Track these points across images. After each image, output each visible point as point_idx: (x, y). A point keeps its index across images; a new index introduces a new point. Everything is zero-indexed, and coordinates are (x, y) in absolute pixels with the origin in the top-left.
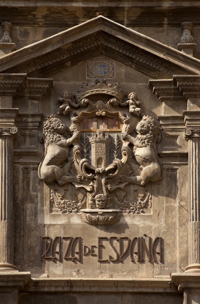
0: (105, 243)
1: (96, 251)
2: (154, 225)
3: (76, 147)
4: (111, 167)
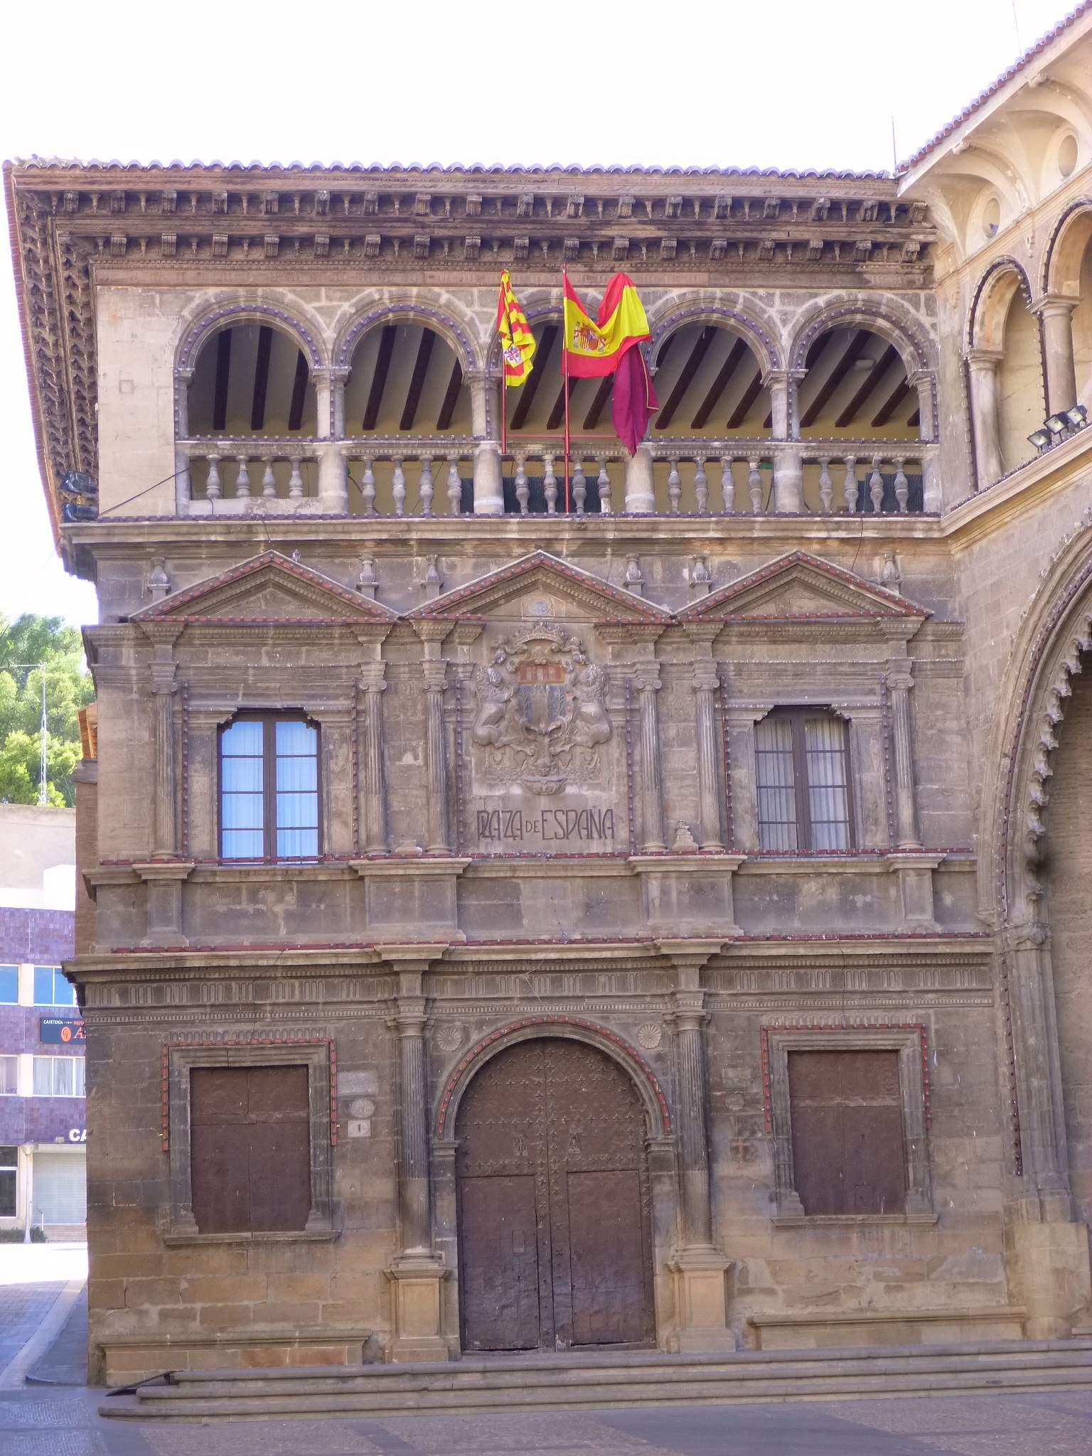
0: (547, 816)
1: (539, 825)
2: (604, 795)
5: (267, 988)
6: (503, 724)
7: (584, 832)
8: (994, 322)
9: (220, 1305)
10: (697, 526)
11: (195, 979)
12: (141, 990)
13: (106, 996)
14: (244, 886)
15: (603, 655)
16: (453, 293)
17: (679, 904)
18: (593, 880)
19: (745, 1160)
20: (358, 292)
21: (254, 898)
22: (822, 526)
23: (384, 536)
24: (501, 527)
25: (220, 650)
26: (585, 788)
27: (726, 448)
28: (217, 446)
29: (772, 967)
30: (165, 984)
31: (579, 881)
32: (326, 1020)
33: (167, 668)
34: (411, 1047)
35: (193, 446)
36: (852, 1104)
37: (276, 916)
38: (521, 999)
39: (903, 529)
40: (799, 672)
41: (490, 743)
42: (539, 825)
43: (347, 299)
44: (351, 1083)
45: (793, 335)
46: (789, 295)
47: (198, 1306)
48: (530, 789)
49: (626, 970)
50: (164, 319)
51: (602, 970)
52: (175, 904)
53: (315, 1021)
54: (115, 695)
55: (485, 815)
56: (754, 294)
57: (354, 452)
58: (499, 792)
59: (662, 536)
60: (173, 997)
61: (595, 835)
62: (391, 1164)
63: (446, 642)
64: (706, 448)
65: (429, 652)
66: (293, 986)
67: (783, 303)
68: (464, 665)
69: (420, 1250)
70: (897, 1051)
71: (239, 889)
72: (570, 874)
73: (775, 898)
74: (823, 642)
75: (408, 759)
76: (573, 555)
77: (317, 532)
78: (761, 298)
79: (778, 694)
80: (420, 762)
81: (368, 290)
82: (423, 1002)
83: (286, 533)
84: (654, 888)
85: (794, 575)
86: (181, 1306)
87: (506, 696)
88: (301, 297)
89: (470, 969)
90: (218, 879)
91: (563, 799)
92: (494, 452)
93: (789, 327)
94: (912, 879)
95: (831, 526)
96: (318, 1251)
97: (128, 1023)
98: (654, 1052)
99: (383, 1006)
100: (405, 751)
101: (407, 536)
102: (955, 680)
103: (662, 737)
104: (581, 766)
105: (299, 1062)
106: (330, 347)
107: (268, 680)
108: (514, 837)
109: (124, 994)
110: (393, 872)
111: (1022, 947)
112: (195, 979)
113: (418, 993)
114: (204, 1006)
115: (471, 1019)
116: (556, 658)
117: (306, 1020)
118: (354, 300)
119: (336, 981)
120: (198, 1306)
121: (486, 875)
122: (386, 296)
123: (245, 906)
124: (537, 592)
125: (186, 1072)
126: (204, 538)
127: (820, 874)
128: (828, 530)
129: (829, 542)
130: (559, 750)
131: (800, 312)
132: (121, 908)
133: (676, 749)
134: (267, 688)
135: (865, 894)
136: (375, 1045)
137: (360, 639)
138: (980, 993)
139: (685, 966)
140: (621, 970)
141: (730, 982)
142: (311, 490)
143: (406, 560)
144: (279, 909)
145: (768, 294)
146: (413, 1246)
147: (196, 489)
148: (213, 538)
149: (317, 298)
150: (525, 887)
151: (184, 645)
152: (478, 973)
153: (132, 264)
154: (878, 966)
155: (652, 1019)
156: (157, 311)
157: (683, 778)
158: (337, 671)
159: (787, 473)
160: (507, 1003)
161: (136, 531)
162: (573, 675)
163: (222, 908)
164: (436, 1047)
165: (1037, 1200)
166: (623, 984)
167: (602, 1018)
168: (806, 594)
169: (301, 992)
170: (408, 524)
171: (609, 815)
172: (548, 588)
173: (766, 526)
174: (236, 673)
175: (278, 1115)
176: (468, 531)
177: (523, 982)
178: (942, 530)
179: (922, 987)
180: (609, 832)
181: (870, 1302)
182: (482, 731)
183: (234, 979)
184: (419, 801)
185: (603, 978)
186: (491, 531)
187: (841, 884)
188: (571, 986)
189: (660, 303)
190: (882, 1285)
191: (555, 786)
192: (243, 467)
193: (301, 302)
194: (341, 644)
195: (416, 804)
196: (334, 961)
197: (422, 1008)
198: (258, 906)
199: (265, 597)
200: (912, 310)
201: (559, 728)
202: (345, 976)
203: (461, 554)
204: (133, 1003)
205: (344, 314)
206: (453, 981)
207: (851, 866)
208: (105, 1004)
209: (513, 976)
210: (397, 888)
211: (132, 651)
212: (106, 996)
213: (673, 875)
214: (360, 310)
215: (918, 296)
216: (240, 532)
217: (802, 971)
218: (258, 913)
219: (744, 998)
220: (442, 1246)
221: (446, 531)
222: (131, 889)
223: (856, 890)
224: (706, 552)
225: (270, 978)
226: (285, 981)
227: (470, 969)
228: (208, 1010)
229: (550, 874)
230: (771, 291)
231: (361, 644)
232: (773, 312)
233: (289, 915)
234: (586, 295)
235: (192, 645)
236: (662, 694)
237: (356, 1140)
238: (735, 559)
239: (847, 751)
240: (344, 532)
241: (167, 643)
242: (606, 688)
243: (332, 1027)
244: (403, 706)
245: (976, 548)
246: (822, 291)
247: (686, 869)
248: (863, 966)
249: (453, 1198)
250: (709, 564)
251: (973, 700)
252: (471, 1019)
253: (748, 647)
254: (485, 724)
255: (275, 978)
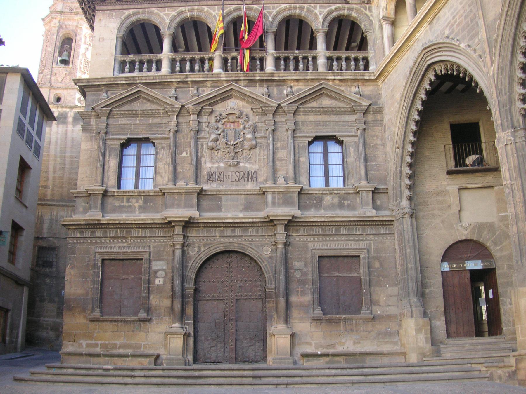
0: (233, 174)
1: (230, 177)
2: (254, 167)
3: (222, 134)
4: (236, 142)
5: (130, 231)
6: (218, 142)
7: (246, 179)
8: (390, 8)
9: (107, 342)
10: (288, 75)
11: (105, 228)
12: (87, 232)
13: (75, 233)
14: (125, 197)
15: (254, 119)
16: (209, 8)
17: (278, 203)
18: (248, 196)
19: (301, 295)
20: (178, 9)
21: (128, 201)
22: (331, 74)
23: (179, 80)
24: (219, 75)
25: (123, 119)
26: (247, 164)
27: (300, 53)
28: (129, 57)
29: (313, 226)
30: (95, 230)
31: (243, 196)
32: (150, 243)
33: (103, 124)
34: (178, 252)
35: (121, 57)
36: (342, 275)
37: (135, 207)
38: (220, 236)
39: (361, 76)
40: (325, 124)
41: (213, 149)
42: (230, 177)
43: (174, 11)
44: (156, 265)
45: (324, 18)
46: (322, 6)
47: (100, 342)
48: (227, 164)
49: (258, 226)
50: (115, 19)
51: (250, 226)
52: (100, 202)
53: (146, 243)
54: (88, 134)
55: (210, 173)
56: (310, 6)
57: (175, 57)
58: (216, 165)
59: (276, 78)
60: (98, 234)
61: (250, 180)
62: (170, 294)
63: (199, 114)
64: (294, 53)
65: (194, 117)
66: (139, 231)
67: (320, 8)
68: (205, 122)
69: (177, 325)
70: (359, 256)
71: (123, 198)
72: (240, 193)
73: (315, 202)
74: (334, 114)
75: (184, 154)
76: (245, 86)
77: (155, 79)
78: (312, 7)
79: (317, 132)
80: (188, 155)
81: (181, 8)
82: (182, 236)
83: (146, 79)
84: (270, 197)
85: (323, 92)
86: (93, 342)
87: (219, 132)
88: (159, 11)
89: (202, 226)
90: (116, 194)
91: (239, 168)
92: (220, 55)
93: (322, 15)
94: (364, 194)
95: (336, 74)
96: (142, 325)
97: (82, 243)
98: (268, 256)
99: (170, 238)
100: (183, 152)
101: (187, 80)
102: (381, 127)
103: (275, 146)
104: (246, 157)
105: (140, 257)
106: (168, 25)
107: (138, 129)
108: (221, 181)
109: (81, 233)
110: (175, 191)
111: (404, 216)
112: (105, 228)
113: (181, 233)
114: (107, 237)
115: (202, 243)
116: (237, 120)
117: (142, 243)
118: (176, 11)
119: (154, 229)
120: (100, 342)
121: (209, 193)
122: (187, 9)
123: (125, 204)
124: (232, 99)
125: (100, 260)
126: (119, 82)
127: (331, 193)
128: (334, 76)
129: (335, 81)
130: (237, 151)
131: (325, 11)
132: (83, 204)
133: (280, 150)
134: (138, 131)
135: (348, 200)
136: (166, 252)
137: (169, 114)
138: (390, 235)
139: (279, 224)
140: (257, 226)
141: (297, 231)
142: (158, 69)
143: (187, 89)
144: (136, 205)
145: (315, 6)
146: (175, 323)
147: (122, 70)
148: (122, 82)
149: (165, 11)
150: (224, 198)
151: (111, 118)
152: (204, 227)
153: (107, 4)
154: (352, 225)
155: (268, 244)
156: (113, 17)
157: (282, 160)
158: (162, 125)
159: (321, 61)
160: (215, 238)
161: (97, 81)
162: (243, 125)
163: (117, 205)
164: (188, 253)
165: (410, 309)
166: (258, 231)
167: (249, 243)
168: (327, 99)
169: (142, 233)
170: (187, 75)
171: (255, 173)
172: (236, 97)
173: (312, 74)
174: (127, 126)
175: (132, 276)
176: (207, 77)
177: (220, 230)
178: (374, 76)
179: (368, 233)
180: (255, 179)
181: (347, 348)
182: (210, 144)
183: (118, 228)
184: (187, 168)
185: (250, 230)
186: (215, 77)
187: (339, 197)
188: (238, 232)
189: (278, 9)
190: (352, 342)
191: (236, 163)
192: (137, 63)
193: (159, 12)
194: (163, 116)
195: (186, 169)
196: (152, 222)
197: (182, 239)
198: (130, 204)
199: (139, 102)
200: (364, 11)
201: (238, 143)
202: (157, 228)
203: (206, 87)
204: (84, 236)
205: (173, 15)
206: (195, 230)
207: (343, 191)
208: (75, 236)
209: (217, 229)
210: (176, 197)
211: (94, 120)
212: (75, 233)
213: (276, 192)
214: (179, 14)
215: (366, 7)
216: (130, 80)
217: (324, 227)
218: (129, 207)
219: (301, 237)
220: (187, 324)
221: (200, 77)
222: (87, 198)
223: (344, 199)
224: (292, 85)
225: (131, 228)
226: (136, 229)
227: (202, 226)
228: (109, 239)
229: (232, 193)
230: (316, 5)
231: (169, 116)
232: (317, 11)
233: (140, 207)
234: (253, 7)
235: (114, 118)
236: (275, 132)
237: (157, 285)
238: (302, 87)
239: (342, 152)
240: (165, 79)
241: (105, 116)
242: (255, 130)
243: (152, 245)
244: (184, 137)
245: (386, 80)
246: (333, 5)
247: (281, 190)
248: (346, 225)
249: (192, 307)
250: (293, 89)
251: (387, 132)
252: (202, 243)
253: (307, 116)
254: (211, 141)
255: (133, 228)
